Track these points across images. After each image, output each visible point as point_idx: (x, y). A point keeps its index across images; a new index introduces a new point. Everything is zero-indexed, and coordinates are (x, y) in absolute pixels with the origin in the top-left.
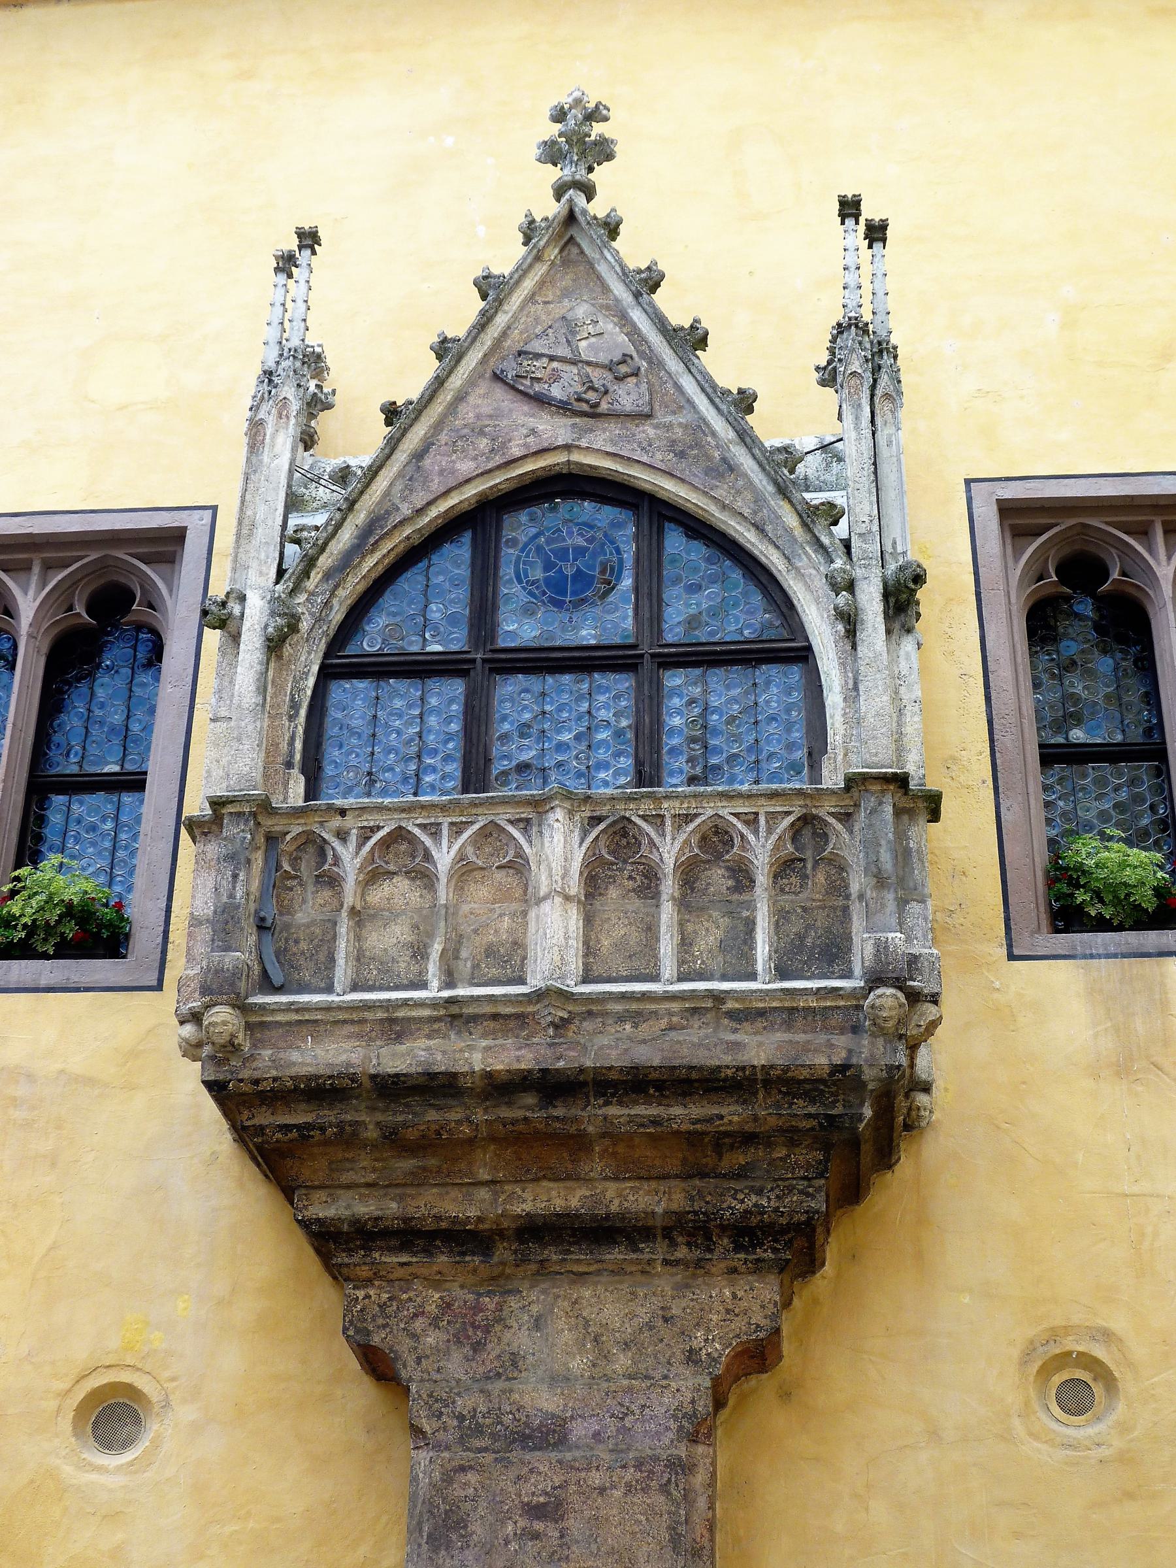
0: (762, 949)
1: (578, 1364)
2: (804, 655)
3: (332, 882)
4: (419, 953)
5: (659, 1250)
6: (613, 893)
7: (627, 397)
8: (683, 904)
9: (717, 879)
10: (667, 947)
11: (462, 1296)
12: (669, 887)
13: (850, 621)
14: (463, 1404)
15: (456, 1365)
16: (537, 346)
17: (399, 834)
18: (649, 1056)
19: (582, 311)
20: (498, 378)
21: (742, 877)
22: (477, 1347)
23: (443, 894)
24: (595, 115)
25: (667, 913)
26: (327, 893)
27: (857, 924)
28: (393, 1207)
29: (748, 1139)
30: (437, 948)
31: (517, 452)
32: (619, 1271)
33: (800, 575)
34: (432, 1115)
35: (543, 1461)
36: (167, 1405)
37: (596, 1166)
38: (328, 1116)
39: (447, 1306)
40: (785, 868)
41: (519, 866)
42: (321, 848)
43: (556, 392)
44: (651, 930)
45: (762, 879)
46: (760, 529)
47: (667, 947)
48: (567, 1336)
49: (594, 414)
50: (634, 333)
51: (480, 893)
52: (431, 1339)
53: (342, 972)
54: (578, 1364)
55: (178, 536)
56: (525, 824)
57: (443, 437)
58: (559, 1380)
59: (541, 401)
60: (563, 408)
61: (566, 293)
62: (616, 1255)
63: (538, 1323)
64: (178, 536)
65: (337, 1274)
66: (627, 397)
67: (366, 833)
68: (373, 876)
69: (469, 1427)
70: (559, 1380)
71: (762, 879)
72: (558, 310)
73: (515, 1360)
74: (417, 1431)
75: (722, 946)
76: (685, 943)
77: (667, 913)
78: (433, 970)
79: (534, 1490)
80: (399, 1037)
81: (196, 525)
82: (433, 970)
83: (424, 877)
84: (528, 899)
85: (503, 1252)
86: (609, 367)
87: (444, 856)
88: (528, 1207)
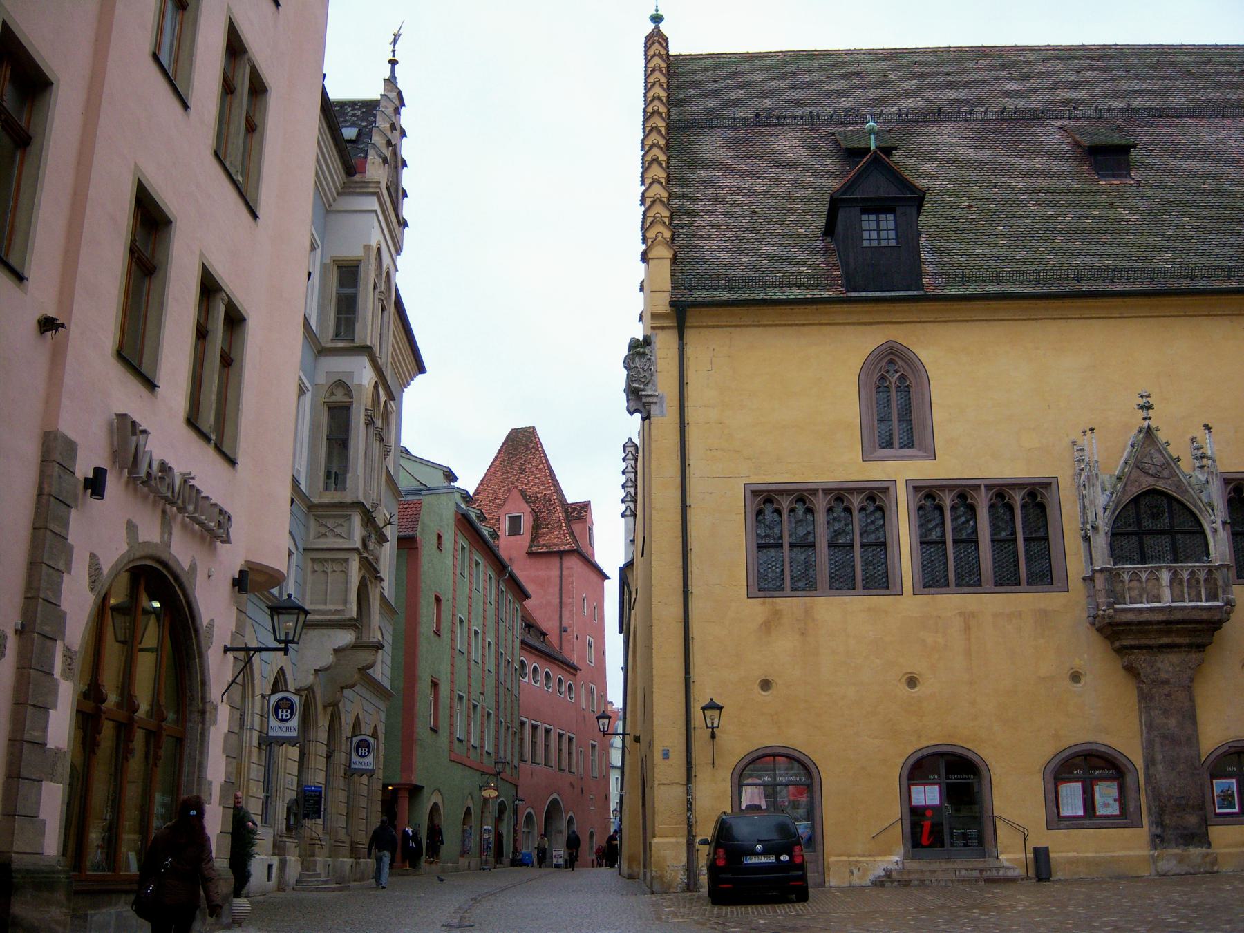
0: (1203, 597)
1: (1170, 669)
2: (1203, 533)
3: (1122, 582)
4: (1141, 596)
5: (1183, 649)
6: (1175, 584)
7: (1166, 473)
8: (1188, 587)
9: (1193, 582)
10: (1186, 596)
11: (1148, 657)
12: (1185, 584)
13: (1215, 531)
14: (1151, 677)
15: (1149, 670)
16: (1145, 460)
17: (1135, 572)
18: (1187, 618)
19: (1153, 451)
20: (1138, 467)
21: (1198, 581)
22: (1152, 666)
23: (1144, 585)
24: (1149, 396)
25: (1186, 590)
26: (1121, 585)
27: (1220, 591)
28: (1137, 643)
29: (1200, 631)
30: (1145, 596)
31: (1144, 486)
32: (1176, 652)
33: (1204, 518)
34: (1146, 627)
35: (1166, 686)
36: (1086, 674)
37: (1174, 635)
38: (1128, 628)
39: (1145, 659)
40: (1206, 580)
41: (1158, 579)
42: (1119, 575)
43: (1151, 472)
44: (1182, 592)
45: (1202, 582)
46: (1195, 506)
47: (1186, 596)
48: (1168, 665)
49: (1159, 477)
50: (1163, 456)
51: (1150, 584)
52: (1143, 665)
53: (1128, 600)
54: (1170, 669)
55: (1050, 484)
56: (1157, 571)
57: (1129, 482)
58: (1167, 672)
59: (1148, 474)
60: (1152, 476)
61: (1149, 446)
62: (1176, 650)
63: (1162, 662)
64: (1050, 484)
65: (1121, 651)
66: (1166, 473)
67: (1128, 572)
68: (1130, 581)
69: (1153, 681)
70: (1167, 672)
71: (1202, 582)
72: (1148, 449)
73: (1159, 669)
74: (1143, 681)
75: (1196, 595)
76: (1189, 595)
77: (1186, 590)
78: (1144, 600)
79: (1166, 691)
80: (1141, 614)
81: (1054, 481)
82: (1144, 600)
83: (1140, 581)
84: (1160, 586)
85: (1155, 650)
86: (1161, 466)
87: (1144, 577)
88: (1161, 642)
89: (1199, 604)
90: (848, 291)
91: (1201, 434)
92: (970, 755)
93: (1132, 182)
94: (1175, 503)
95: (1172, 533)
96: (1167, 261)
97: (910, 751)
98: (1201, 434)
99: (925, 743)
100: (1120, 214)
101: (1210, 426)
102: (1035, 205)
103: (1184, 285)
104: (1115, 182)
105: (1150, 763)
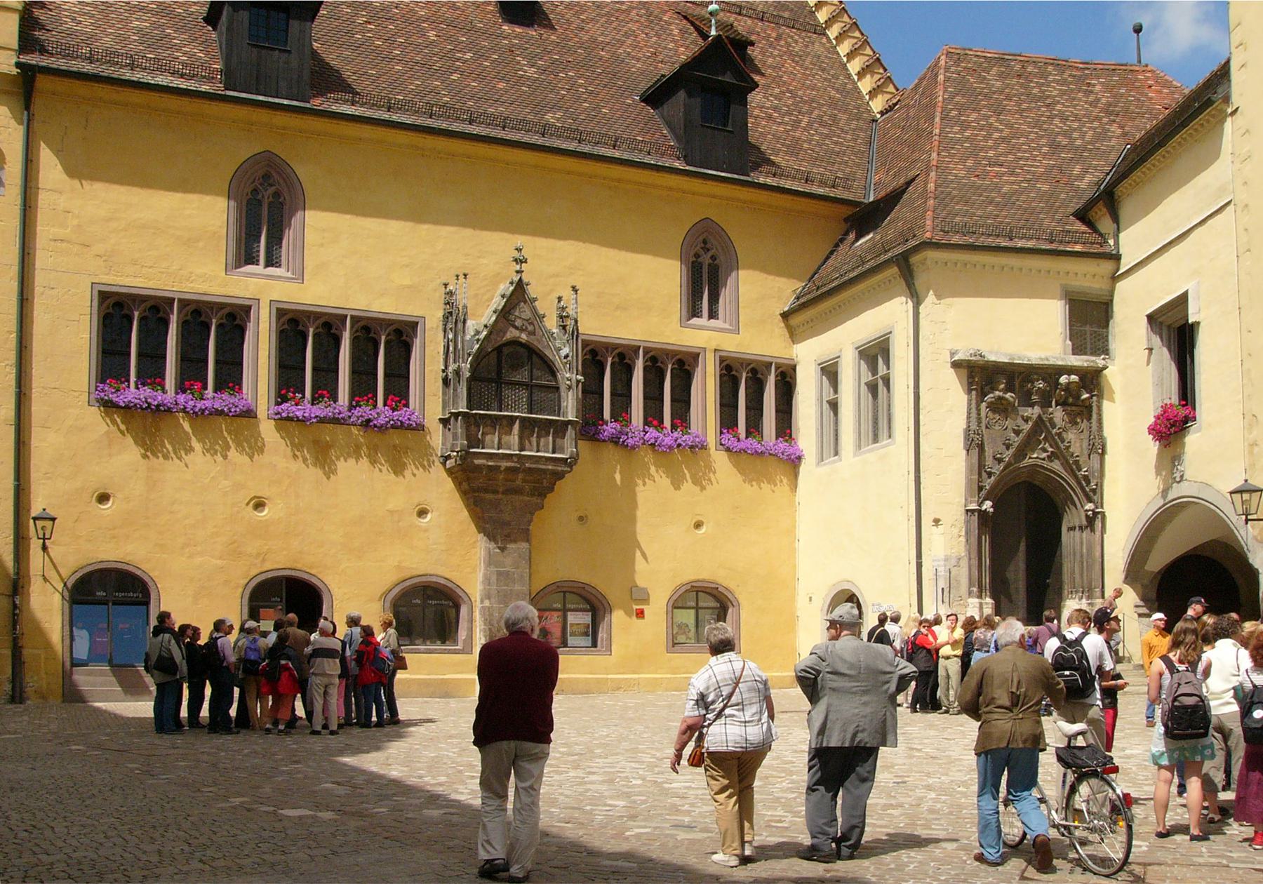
89: (546, 455)
90: (226, 89)
91: (567, 294)
92: (314, 580)
93: (534, 33)
94: (534, 357)
95: (529, 387)
96: (558, 119)
97: (254, 572)
98: (567, 294)
99: (268, 566)
100: (518, 63)
101: (577, 288)
102: (436, 36)
103: (573, 146)
104: (518, 30)
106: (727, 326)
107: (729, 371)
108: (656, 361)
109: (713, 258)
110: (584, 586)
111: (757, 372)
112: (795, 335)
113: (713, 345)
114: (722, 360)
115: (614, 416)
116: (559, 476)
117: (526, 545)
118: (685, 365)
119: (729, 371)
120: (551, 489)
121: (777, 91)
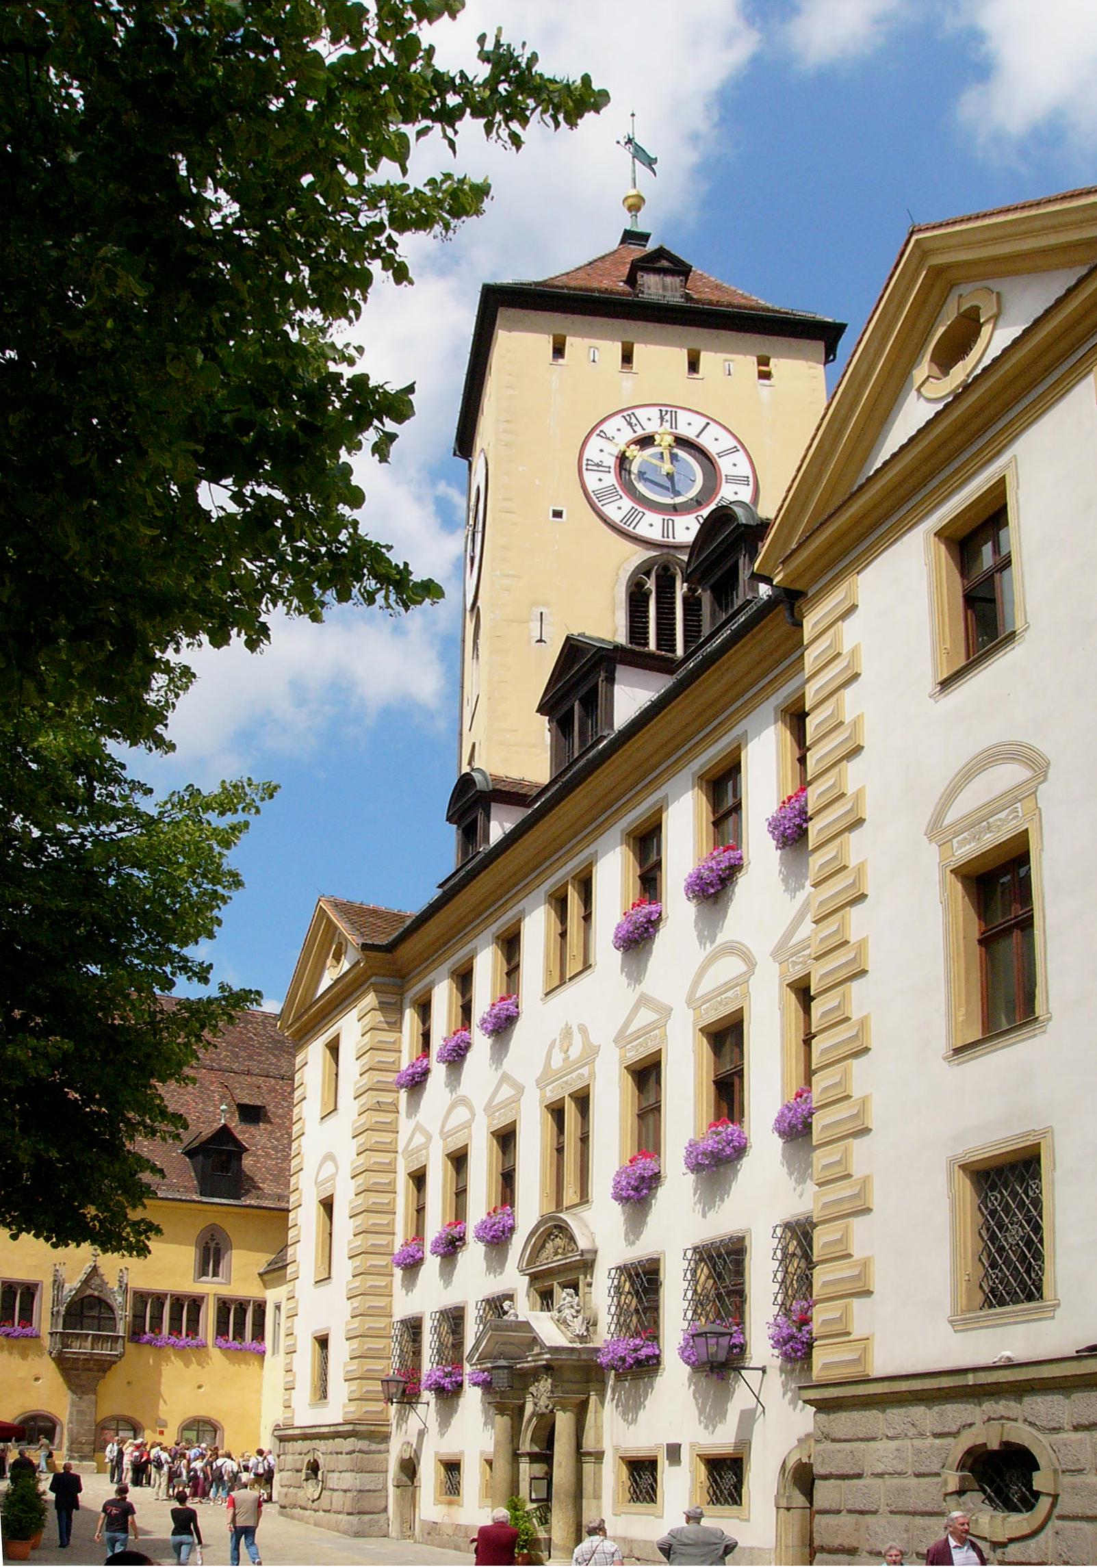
105: (71, 1422)
106: (223, 1281)
107: (224, 1306)
108: (178, 1301)
109: (217, 1244)
110: (129, 1418)
111: (242, 1306)
112: (266, 1285)
113: (214, 1292)
114: (219, 1299)
115: (152, 1330)
116: (115, 1363)
117: (94, 1397)
118: (196, 1303)
119: (224, 1306)
120: (110, 1369)
121: (279, 1134)
